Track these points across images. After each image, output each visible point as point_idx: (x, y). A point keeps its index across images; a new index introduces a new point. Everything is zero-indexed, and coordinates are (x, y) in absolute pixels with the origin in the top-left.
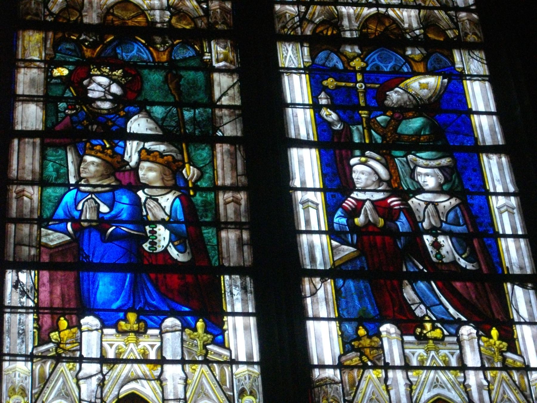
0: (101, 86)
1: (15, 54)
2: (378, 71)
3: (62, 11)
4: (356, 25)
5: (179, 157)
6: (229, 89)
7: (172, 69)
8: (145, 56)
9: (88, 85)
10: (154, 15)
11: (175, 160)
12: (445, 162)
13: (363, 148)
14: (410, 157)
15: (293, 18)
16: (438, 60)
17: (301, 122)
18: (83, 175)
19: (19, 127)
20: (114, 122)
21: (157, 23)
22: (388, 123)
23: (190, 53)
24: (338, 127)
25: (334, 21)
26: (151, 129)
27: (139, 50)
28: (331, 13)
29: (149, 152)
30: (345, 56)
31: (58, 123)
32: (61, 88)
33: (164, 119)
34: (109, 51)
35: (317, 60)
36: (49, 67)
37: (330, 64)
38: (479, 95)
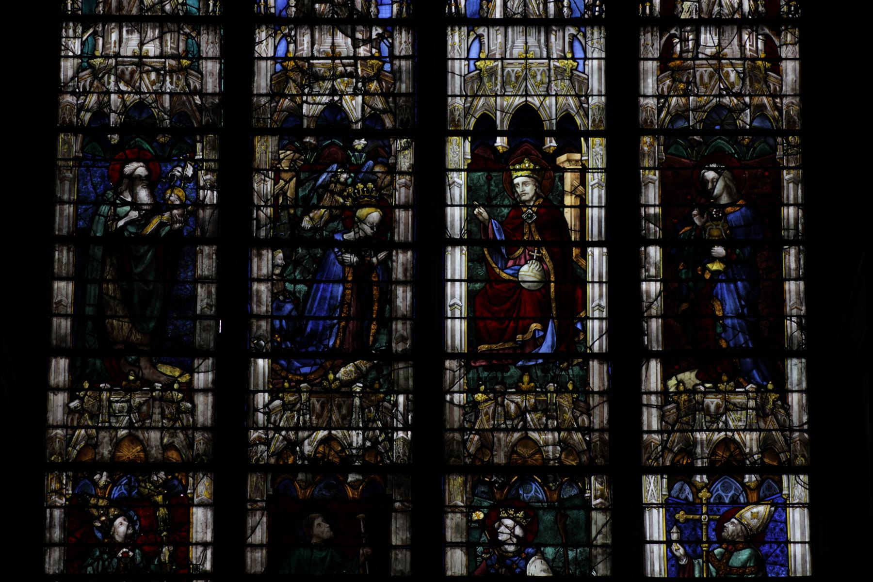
0: (508, 528)
1: (444, 499)
2: (720, 500)
3: (478, 450)
6: (603, 526)
7: (560, 508)
8: (541, 496)
9: (498, 528)
10: (548, 452)
15: (657, 448)
16: (770, 487)
20: (517, 564)
21: (550, 460)
23: (574, 492)
24: (683, 562)
25: (689, 448)
26: (544, 571)
27: (536, 491)
30: (695, 487)
31: (477, 567)
32: (478, 531)
33: (553, 560)
34: (513, 492)
35: (673, 492)
36: (469, 511)
37: (683, 497)
38: (798, 523)
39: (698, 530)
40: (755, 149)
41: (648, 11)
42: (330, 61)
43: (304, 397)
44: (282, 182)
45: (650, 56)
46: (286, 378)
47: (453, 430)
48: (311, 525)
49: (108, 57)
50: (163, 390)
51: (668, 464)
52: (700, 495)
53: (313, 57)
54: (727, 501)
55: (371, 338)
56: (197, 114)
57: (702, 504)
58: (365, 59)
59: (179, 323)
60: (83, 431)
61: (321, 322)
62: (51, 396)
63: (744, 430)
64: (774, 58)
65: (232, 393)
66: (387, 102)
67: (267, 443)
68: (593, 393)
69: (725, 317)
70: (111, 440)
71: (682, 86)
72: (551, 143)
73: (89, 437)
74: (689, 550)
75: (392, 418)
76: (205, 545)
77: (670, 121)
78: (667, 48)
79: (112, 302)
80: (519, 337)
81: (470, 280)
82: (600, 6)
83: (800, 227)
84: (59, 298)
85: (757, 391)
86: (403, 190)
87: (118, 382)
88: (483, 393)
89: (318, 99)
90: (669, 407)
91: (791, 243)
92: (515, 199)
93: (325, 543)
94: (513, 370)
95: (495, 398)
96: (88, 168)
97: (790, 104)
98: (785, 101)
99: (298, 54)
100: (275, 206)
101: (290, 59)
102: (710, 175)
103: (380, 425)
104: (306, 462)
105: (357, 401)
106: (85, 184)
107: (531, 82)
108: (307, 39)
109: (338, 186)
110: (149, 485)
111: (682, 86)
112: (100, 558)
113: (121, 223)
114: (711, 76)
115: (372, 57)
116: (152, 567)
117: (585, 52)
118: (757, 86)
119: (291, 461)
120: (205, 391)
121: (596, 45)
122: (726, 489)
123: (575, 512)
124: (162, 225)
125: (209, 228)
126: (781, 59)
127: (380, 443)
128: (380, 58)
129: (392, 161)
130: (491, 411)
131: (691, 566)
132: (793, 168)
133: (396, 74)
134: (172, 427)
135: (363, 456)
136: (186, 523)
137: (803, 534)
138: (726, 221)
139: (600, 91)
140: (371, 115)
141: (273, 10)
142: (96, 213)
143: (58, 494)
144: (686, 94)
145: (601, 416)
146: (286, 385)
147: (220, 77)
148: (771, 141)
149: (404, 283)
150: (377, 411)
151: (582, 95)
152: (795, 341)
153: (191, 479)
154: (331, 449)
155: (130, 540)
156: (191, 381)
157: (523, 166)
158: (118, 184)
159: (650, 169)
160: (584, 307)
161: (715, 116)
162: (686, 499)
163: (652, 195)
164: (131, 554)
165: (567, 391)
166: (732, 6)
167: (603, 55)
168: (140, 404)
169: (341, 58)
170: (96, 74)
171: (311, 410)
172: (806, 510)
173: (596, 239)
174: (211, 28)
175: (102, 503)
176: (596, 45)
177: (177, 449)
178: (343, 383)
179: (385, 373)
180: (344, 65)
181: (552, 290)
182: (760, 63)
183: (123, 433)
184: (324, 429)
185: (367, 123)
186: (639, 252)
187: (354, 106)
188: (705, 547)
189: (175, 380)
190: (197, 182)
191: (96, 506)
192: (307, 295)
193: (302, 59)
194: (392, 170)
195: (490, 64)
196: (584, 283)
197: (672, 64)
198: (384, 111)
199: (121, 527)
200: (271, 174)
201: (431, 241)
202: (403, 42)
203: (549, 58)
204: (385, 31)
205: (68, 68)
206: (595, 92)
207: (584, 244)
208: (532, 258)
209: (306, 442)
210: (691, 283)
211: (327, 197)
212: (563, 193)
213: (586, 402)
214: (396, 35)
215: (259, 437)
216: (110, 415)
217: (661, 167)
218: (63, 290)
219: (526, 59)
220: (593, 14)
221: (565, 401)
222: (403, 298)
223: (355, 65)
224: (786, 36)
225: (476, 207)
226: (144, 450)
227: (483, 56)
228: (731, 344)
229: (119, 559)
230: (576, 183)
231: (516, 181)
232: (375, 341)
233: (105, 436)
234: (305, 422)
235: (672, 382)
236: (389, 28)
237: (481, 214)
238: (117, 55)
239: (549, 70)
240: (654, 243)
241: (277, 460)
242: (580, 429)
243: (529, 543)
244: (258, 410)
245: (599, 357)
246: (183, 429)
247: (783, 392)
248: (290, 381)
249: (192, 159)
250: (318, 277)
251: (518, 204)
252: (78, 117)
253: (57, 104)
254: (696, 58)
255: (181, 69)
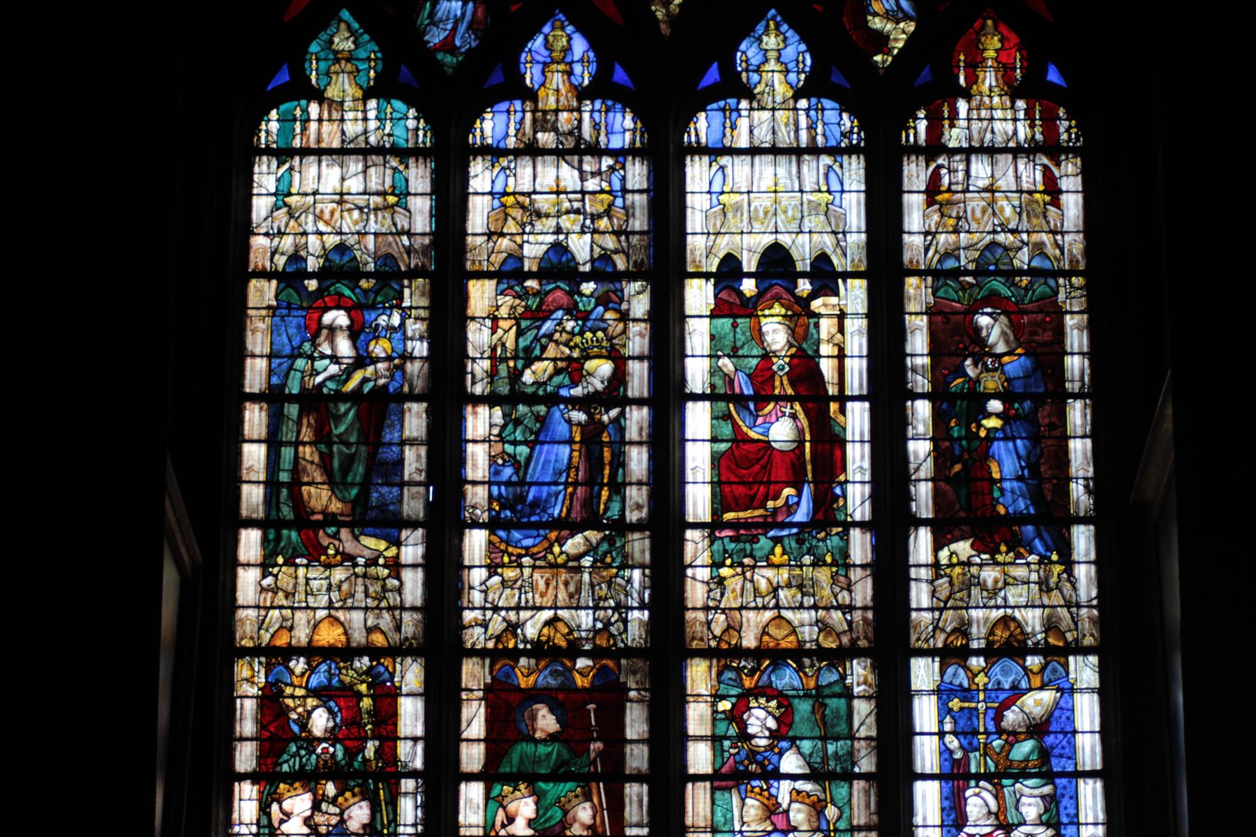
0: (760, 720)
1: (685, 688)
3: (723, 633)
4: (984, 631)
5: (822, 797)
7: (818, 696)
11: (819, 800)
12: (1047, 789)
13: (978, 777)
14: (1018, 786)
16: (1054, 671)
17: (927, 754)
18: (745, 819)
19: (691, 771)
21: (805, 642)
22: (1003, 747)
23: (835, 677)
24: (958, 755)
25: (963, 630)
28: (962, 619)
29: (799, 792)
31: (724, 764)
33: (811, 755)
34: (765, 678)
35: (946, 678)
37: (957, 682)
38: (1087, 712)
39: (975, 720)
40: (1034, 291)
41: (912, 139)
42: (554, 196)
43: (527, 572)
44: (500, 332)
45: (915, 189)
46: (505, 551)
47: (694, 609)
48: (534, 718)
49: (306, 195)
50: (366, 565)
51: (940, 645)
52: (976, 680)
53: (535, 192)
54: (1007, 686)
55: (602, 506)
56: (405, 256)
57: (978, 690)
58: (594, 193)
59: (384, 490)
60: (277, 612)
61: (545, 489)
62: (240, 571)
63: (1026, 607)
64: (1053, 190)
65: (444, 569)
66: (619, 241)
67: (485, 625)
68: (855, 566)
69: (1002, 480)
70: (309, 622)
71: (952, 222)
72: (804, 286)
73: (284, 619)
74: (965, 743)
75: (626, 596)
76: (415, 739)
77: (939, 261)
78: (935, 178)
79: (309, 466)
80: (770, 504)
81: (714, 440)
82: (859, 134)
83: (1086, 379)
84: (250, 463)
85: (1040, 563)
86: (637, 339)
87: (314, 554)
88: (731, 566)
89: (540, 238)
90: (940, 581)
91: (1075, 396)
92: (764, 349)
93: (552, 738)
94: (763, 540)
95: (743, 573)
96: (282, 317)
97: (1074, 243)
98: (1068, 238)
99: (519, 189)
100: (493, 358)
101: (509, 194)
102: (984, 321)
103: (612, 603)
104: (529, 646)
105: (586, 577)
106: (279, 335)
107: (781, 218)
108: (529, 170)
109: (564, 335)
110: (351, 673)
111: (952, 222)
112: (297, 754)
113: (319, 379)
114: (984, 212)
115: (602, 191)
116: (356, 764)
117: (842, 184)
118: (1035, 221)
119: (511, 645)
120: (414, 566)
121: (854, 177)
122: (1005, 673)
123: (835, 700)
124: (365, 380)
125: (419, 385)
126: (1061, 192)
127: (612, 624)
128: (610, 193)
129: (624, 306)
130: (738, 588)
131: (966, 759)
132: (1077, 313)
133: (628, 211)
134: (377, 607)
135: (594, 638)
136: (393, 715)
137: (1092, 722)
138: (1003, 373)
139: (859, 227)
140: (601, 256)
141: (490, 141)
142: (291, 368)
143: (249, 680)
144: (956, 231)
145: (863, 591)
146: (506, 559)
147: (431, 216)
148: (1052, 282)
149: (640, 443)
150: (609, 588)
151: (839, 233)
152: (1082, 507)
153: (398, 667)
154: (556, 630)
155: (332, 736)
156: (398, 556)
157: (773, 311)
158: (316, 335)
159: (916, 314)
160: (844, 469)
161: (988, 254)
162: (961, 685)
163: (918, 342)
164: (331, 750)
165: (825, 564)
166: (1006, 133)
167: (863, 188)
168: (341, 582)
169: (566, 193)
170: (291, 215)
171: (533, 587)
172: (1096, 696)
173: (856, 393)
174: (421, 160)
175: (299, 692)
176: (854, 177)
177: (383, 632)
178: (570, 558)
179: (618, 544)
180: (570, 201)
181: (808, 449)
182: (1037, 196)
183: (321, 614)
184: (550, 608)
185: (597, 264)
186: (905, 408)
187: (581, 247)
188: (982, 738)
189: (380, 554)
190: (405, 333)
191: (293, 697)
192: (529, 459)
193: (523, 194)
194: (624, 317)
195: (735, 198)
196: (843, 443)
197: (939, 198)
198: (616, 252)
199: (320, 721)
200: (488, 322)
201: (668, 396)
202: (637, 174)
203: (801, 191)
204: (617, 162)
205: (261, 206)
206: (854, 229)
207: (842, 399)
208: (784, 414)
209: (529, 623)
210: (964, 443)
211: (552, 346)
212: (818, 342)
213: (846, 576)
214: (629, 165)
215: (476, 619)
216: (307, 594)
217: (930, 312)
218: (254, 455)
219: (775, 192)
220: (851, 142)
221: (823, 575)
222: (638, 461)
223: (583, 200)
224: (1066, 166)
225: (719, 357)
226: (346, 633)
227: (726, 189)
228: (1011, 510)
229: (318, 756)
230: (834, 330)
231: (764, 329)
232: (606, 509)
233: (301, 617)
234: (527, 601)
235: (944, 555)
236: (621, 159)
237: (726, 366)
238: (315, 193)
239: (802, 204)
240: (922, 396)
241: (496, 644)
242: (839, 607)
243: (782, 735)
244: (471, 588)
245: (862, 525)
246: (390, 609)
247: (1068, 562)
248: (510, 555)
249: (399, 307)
250: (541, 438)
251: (767, 357)
252: (272, 261)
253: (247, 247)
254: (966, 191)
255: (387, 207)
